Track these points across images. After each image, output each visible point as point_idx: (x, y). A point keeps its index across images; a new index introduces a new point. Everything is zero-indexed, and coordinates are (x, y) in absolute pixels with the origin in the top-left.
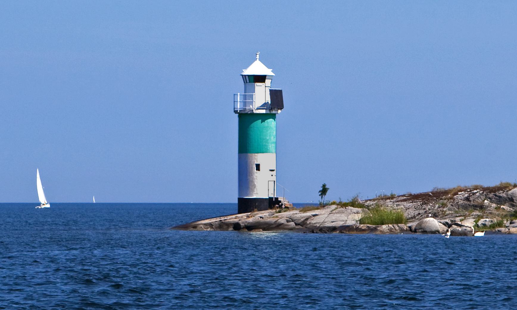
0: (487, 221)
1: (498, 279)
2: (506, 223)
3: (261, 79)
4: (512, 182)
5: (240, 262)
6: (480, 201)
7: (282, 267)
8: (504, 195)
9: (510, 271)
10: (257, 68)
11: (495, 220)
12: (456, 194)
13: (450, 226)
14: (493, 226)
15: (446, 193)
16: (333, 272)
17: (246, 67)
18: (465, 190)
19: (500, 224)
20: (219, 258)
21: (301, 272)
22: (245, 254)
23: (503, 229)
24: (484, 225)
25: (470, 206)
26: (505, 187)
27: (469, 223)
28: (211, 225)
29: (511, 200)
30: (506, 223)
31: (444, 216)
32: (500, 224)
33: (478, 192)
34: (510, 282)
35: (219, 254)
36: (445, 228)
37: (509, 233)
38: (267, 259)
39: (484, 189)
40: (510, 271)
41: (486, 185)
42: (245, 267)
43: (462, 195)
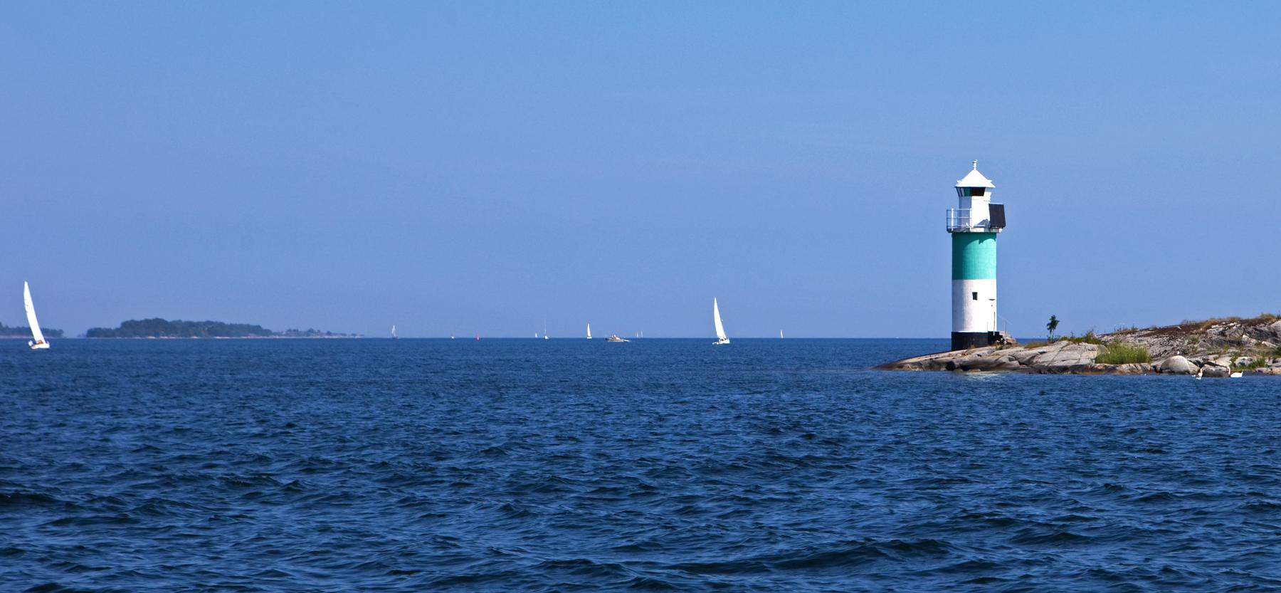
0: (1246, 359)
1: (1259, 428)
2: (1268, 362)
3: (979, 191)
4: (1275, 314)
5: (954, 408)
6: (1237, 336)
7: (1003, 413)
8: (1266, 329)
9: (1273, 419)
10: (974, 179)
11: (1255, 359)
12: (1209, 327)
13: (1201, 365)
14: (1253, 366)
15: (1197, 326)
16: (1064, 420)
17: (961, 178)
18: (1220, 323)
19: (1261, 364)
20: (928, 403)
21: (1026, 420)
22: (960, 398)
23: (1264, 369)
24: (1242, 364)
25: (1227, 342)
26: (1267, 320)
27: (1224, 362)
28: (919, 364)
29: (1273, 335)
30: (1268, 362)
31: (1195, 353)
32: (1261, 364)
33: (1235, 326)
34: (1273, 431)
35: (929, 398)
36: (1197, 368)
37: (1272, 374)
38: (986, 405)
39: (1242, 322)
40: (1273, 419)
41: (1244, 318)
42: (960, 414)
43: (1216, 329)
